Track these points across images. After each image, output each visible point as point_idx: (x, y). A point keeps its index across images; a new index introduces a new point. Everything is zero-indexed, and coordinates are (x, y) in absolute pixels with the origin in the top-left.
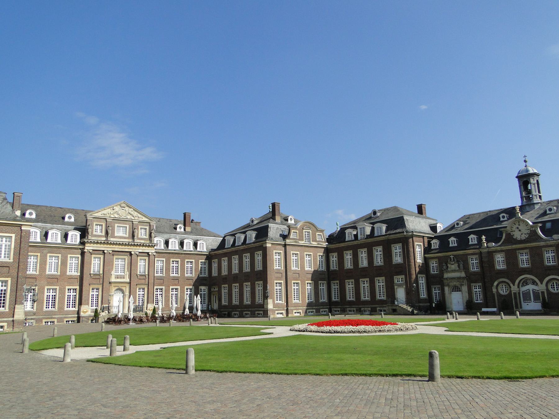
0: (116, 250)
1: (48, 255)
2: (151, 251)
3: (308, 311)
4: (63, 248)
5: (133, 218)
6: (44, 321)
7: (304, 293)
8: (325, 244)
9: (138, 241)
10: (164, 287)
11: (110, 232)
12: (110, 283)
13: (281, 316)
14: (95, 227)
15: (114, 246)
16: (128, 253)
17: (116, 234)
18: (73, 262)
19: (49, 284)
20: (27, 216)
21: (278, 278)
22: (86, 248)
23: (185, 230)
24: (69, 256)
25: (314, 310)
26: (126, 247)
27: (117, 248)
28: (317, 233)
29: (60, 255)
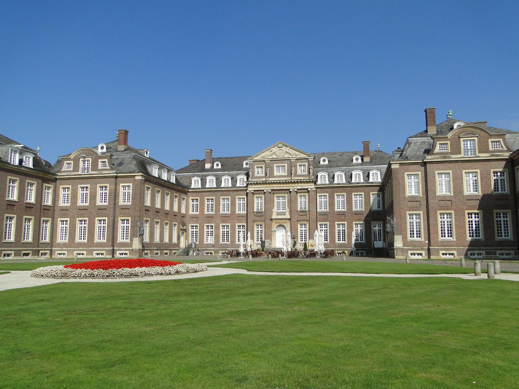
0: (275, 188)
1: (221, 197)
2: (311, 187)
3: (469, 253)
4: (234, 190)
5: (290, 156)
6: (220, 252)
7: (460, 227)
8: (507, 155)
9: (297, 178)
10: (328, 223)
11: (268, 173)
12: (271, 220)
13: (420, 257)
14: (256, 170)
15: (273, 185)
16: (288, 191)
17: (276, 173)
19: (223, 222)
20: (215, 167)
21: (411, 209)
22: (249, 189)
23: (362, 160)
24: (237, 197)
25: (484, 252)
26: (285, 185)
27: (276, 187)
28: (490, 140)
29: (230, 197)
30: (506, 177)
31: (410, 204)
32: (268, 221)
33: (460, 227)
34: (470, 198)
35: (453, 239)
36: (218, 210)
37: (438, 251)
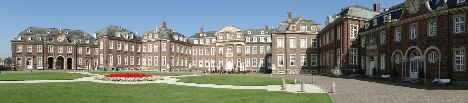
7: (298, 61)
8: (317, 33)
13: (282, 74)
14: (220, 36)
18: (213, 50)
27: (228, 43)
30: (316, 41)
31: (279, 51)
32: (224, 58)
33: (298, 61)
34: (303, 49)
35: (296, 66)
36: (204, 53)
37: (289, 71)
